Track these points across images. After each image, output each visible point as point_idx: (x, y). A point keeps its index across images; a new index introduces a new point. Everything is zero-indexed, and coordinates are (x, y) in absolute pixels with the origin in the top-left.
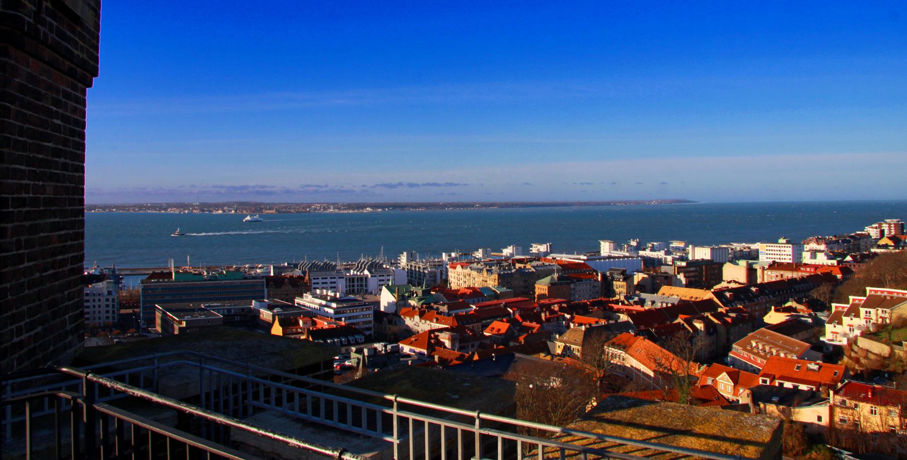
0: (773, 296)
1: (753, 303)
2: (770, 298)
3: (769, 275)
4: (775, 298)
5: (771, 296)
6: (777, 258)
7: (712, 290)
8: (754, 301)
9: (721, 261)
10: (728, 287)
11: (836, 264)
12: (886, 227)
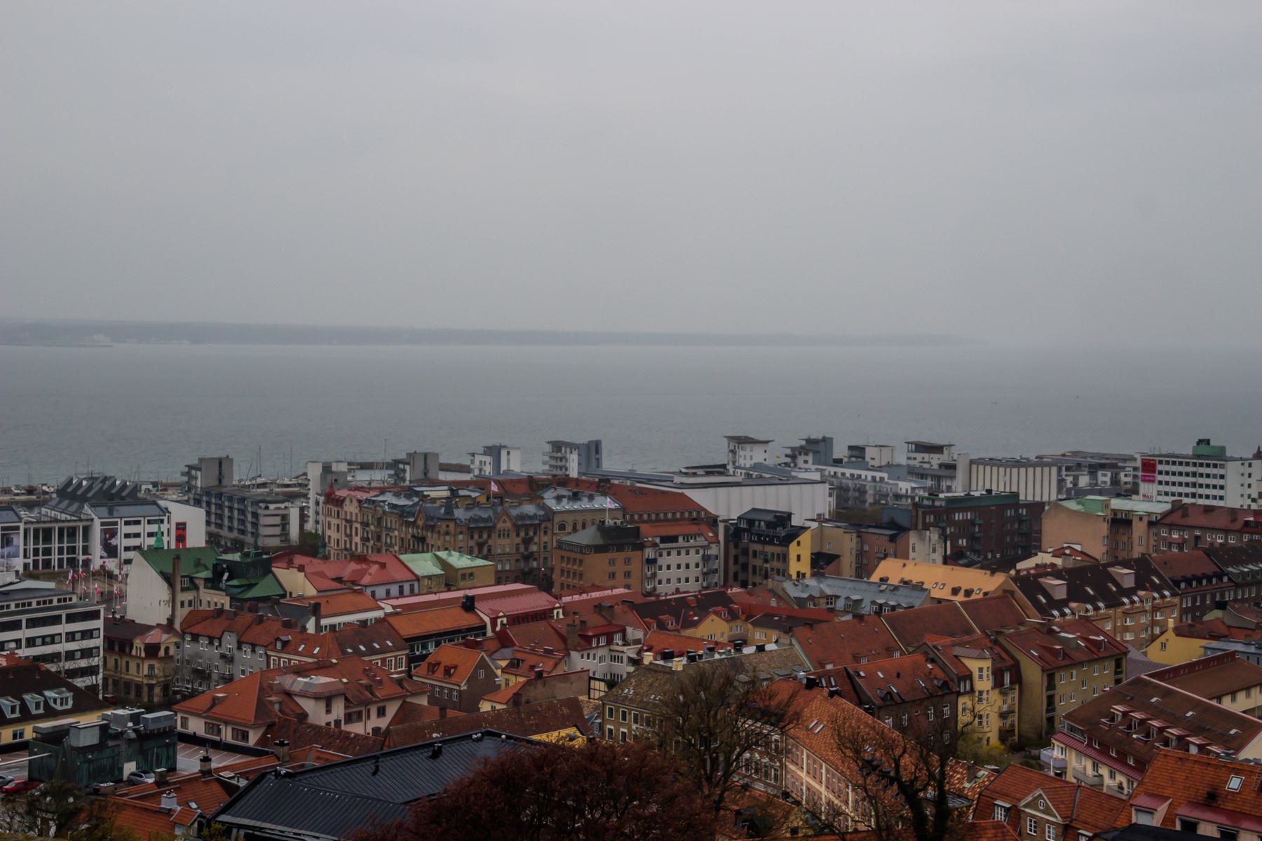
0: (1173, 595)
1: (1119, 610)
2: (1163, 597)
3: (1164, 539)
4: (1176, 600)
5: (1167, 593)
8: (1124, 604)
9: (1038, 499)
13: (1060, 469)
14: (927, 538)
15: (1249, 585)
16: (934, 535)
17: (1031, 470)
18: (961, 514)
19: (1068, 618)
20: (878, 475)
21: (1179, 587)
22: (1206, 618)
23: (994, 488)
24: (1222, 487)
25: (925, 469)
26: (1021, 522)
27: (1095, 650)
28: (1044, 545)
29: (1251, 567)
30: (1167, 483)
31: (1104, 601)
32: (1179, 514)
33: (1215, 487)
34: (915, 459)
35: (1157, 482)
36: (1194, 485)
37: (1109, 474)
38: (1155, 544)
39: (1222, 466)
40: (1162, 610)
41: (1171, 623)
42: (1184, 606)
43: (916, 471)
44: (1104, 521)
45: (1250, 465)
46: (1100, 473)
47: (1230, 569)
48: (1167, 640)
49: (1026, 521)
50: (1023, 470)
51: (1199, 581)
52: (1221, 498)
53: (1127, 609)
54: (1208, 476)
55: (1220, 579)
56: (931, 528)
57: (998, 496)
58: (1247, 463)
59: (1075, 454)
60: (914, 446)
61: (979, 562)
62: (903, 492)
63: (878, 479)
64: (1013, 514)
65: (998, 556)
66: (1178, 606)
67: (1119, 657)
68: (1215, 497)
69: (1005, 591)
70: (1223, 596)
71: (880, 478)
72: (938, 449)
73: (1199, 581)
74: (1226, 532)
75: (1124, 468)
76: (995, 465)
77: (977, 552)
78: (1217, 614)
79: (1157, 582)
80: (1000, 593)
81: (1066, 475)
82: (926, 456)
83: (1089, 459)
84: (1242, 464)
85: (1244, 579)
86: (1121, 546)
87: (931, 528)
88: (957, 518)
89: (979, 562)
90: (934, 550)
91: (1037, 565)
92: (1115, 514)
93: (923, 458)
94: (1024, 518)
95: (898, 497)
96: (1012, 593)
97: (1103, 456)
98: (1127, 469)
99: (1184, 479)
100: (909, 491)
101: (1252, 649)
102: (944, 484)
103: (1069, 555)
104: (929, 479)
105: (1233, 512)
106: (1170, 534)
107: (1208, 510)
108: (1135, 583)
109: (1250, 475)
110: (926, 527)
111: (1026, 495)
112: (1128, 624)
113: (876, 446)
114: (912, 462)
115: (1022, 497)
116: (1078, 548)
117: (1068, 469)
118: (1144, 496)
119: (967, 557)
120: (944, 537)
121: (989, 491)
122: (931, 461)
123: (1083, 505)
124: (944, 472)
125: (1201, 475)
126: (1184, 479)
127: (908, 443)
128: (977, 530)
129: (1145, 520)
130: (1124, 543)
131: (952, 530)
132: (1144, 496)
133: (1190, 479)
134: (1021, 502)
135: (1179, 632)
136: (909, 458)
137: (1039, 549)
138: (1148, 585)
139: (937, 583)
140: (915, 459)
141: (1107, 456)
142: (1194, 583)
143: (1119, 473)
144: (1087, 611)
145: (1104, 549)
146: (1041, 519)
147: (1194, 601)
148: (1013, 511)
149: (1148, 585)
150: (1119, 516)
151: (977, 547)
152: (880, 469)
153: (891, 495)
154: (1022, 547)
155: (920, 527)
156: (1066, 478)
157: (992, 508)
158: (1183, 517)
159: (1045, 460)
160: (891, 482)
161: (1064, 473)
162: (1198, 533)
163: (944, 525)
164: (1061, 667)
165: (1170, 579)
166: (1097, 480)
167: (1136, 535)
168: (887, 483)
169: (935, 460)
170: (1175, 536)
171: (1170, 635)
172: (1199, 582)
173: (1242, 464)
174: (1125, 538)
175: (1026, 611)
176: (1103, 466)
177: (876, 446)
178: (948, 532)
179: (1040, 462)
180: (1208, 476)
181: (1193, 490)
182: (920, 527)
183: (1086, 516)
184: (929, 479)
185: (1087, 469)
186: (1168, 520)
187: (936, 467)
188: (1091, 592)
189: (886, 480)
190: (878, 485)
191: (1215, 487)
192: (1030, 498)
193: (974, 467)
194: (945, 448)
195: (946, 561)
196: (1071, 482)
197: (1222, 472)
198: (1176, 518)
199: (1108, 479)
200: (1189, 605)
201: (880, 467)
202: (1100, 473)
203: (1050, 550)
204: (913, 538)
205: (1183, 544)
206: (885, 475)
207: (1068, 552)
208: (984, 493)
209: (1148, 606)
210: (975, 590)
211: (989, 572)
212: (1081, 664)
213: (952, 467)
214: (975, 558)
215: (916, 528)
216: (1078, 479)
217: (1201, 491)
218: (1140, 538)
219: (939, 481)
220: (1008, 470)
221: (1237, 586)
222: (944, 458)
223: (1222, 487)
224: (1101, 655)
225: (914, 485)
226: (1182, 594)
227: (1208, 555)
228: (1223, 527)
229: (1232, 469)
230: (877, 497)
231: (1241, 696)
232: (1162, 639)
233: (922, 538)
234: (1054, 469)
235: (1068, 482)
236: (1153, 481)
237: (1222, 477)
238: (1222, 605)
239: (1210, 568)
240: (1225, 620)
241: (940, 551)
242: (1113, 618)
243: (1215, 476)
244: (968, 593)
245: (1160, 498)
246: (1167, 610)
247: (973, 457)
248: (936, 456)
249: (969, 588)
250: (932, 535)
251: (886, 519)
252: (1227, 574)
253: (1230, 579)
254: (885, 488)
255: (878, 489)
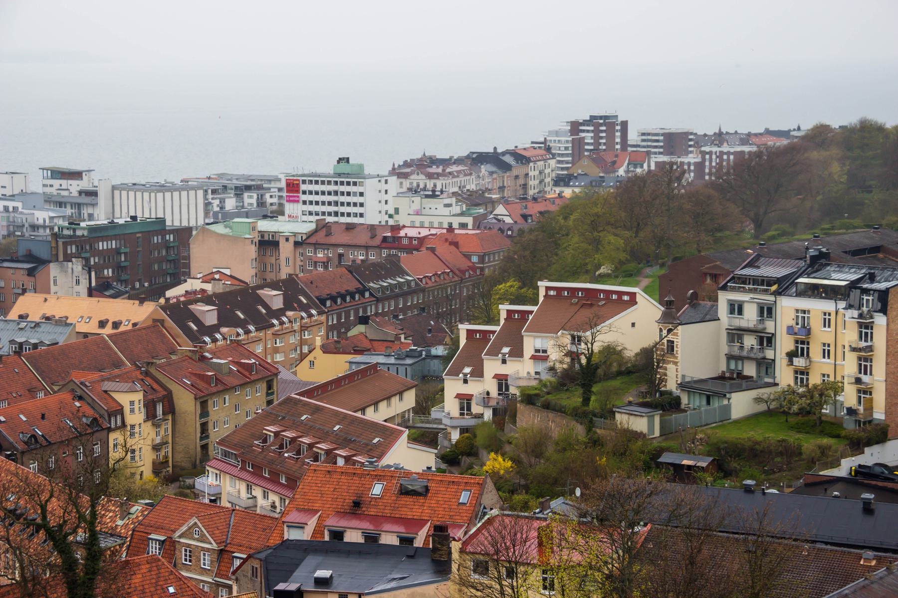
0: (319, 313)
1: (269, 332)
2: (310, 316)
3: (310, 258)
4: (323, 318)
5: (314, 312)
6: (330, 214)
7: (162, 301)
8: (273, 325)
9: (185, 224)
10: (203, 291)
11: (470, 226)
12: (588, 131)
13: (206, 191)
14: (70, 270)
15: (388, 298)
16: (77, 266)
17: (176, 194)
18: (105, 243)
19: (219, 343)
20: (11, 204)
21: (325, 306)
22: (350, 334)
23: (139, 215)
24: (362, 205)
25: (63, 197)
26: (168, 248)
27: (247, 374)
28: (194, 271)
29: (390, 281)
30: (311, 203)
31: (254, 323)
32: (322, 233)
33: (355, 205)
34: (51, 186)
35: (301, 202)
36: (336, 203)
37: (255, 196)
38: (302, 263)
39: (361, 184)
40: (309, 329)
41: (318, 341)
42: (330, 323)
43: (54, 199)
44: (252, 241)
45: (386, 182)
46: (246, 195)
47: (371, 284)
48: (315, 358)
49: (173, 247)
50: (168, 195)
51: (344, 299)
52: (361, 215)
53: (278, 331)
54: (349, 194)
55: (362, 295)
56: (73, 260)
57: (144, 223)
58: (383, 180)
59: (221, 176)
60: (49, 172)
61: (127, 292)
62: (41, 222)
63: (11, 209)
64: (160, 241)
65: (146, 284)
66: (325, 324)
67: (270, 378)
68: (355, 215)
69: (155, 321)
70: (365, 311)
71: (13, 207)
72: (76, 175)
73: (344, 299)
74: (367, 248)
75: (269, 189)
76: (139, 190)
77: (125, 282)
78: (361, 328)
79: (305, 301)
80: (150, 323)
81: (213, 199)
82: (65, 183)
83: (235, 182)
84: (380, 181)
85: (383, 293)
86: (269, 269)
87: (73, 260)
88: (101, 248)
89: (127, 292)
90: (78, 282)
91: (186, 291)
92: (262, 236)
93: (61, 185)
94: (171, 245)
95: (34, 227)
96: (162, 322)
97: (249, 178)
98: (272, 190)
99: (327, 198)
100: (47, 221)
101: (392, 360)
102: (85, 212)
103: (219, 280)
104: (69, 207)
105: (372, 228)
106: (315, 253)
107: (350, 227)
108: (284, 304)
109: (386, 192)
110: (68, 258)
111: (173, 221)
112: (278, 345)
113: (7, 173)
114: (48, 190)
115: (168, 223)
116: (227, 272)
117: (214, 192)
118: (290, 216)
119: (113, 288)
120: (88, 268)
121: (134, 218)
122: (69, 187)
123: (231, 228)
124: (84, 199)
125: (342, 194)
126: (327, 198)
127: (43, 169)
128: (123, 259)
129: (292, 240)
130: (272, 265)
131: (97, 260)
132: (290, 216)
133: (332, 198)
134: (167, 228)
135: (326, 349)
136: (44, 186)
137: (188, 275)
138: (296, 305)
139: (82, 317)
140: (51, 186)
141: (251, 178)
142: (339, 300)
143: (265, 195)
144: (238, 335)
145: (253, 272)
146: (189, 245)
147: (339, 318)
148: (160, 237)
149: (296, 305)
150: (266, 238)
151: (124, 277)
152: (12, 197)
153: (27, 225)
154: (170, 274)
155: (61, 258)
156: (212, 201)
157: (138, 235)
158: (326, 236)
159: (190, 183)
160: (25, 211)
161: (210, 196)
162: (341, 251)
163: (87, 255)
164: (213, 394)
165: (316, 297)
166: (243, 202)
167: (283, 257)
168: (21, 213)
169: (75, 186)
170: (320, 255)
171: (318, 352)
172: (344, 299)
173: (380, 181)
174: (273, 260)
175: (177, 340)
176: (248, 188)
177: (7, 173)
178: (92, 263)
179: (186, 186)
180: (349, 194)
181: (335, 209)
182: (61, 258)
183: (235, 239)
184: (69, 207)
185: (233, 192)
186: (313, 240)
187: (75, 194)
188: (242, 316)
189: (20, 209)
190: (12, 215)
191: (355, 205)
192: (177, 223)
193: (117, 193)
194: (84, 174)
195: (91, 293)
196: (218, 206)
197: (361, 189)
198: (320, 237)
199: (254, 201)
200: (335, 322)
201: (13, 196)
202: (246, 195)
203: (199, 276)
204: (54, 270)
205: (328, 262)
206: (19, 205)
207: (217, 276)
208: (129, 219)
209: (296, 326)
210: (124, 322)
211: (137, 302)
212: (234, 388)
213: (93, 194)
214: (122, 288)
215: (57, 260)
216: (224, 202)
217: (342, 209)
218: (288, 259)
219: (79, 209)
220: (153, 195)
221: (378, 300)
222: (84, 184)
223: (362, 205)
224: (252, 378)
225: (52, 214)
226: (328, 311)
227: (351, 272)
228: (364, 244)
229: (370, 187)
230: (11, 228)
231: (383, 405)
232: (310, 357)
233: (64, 270)
234: (200, 193)
235: (215, 205)
236: (298, 201)
237: (361, 194)
238: (364, 320)
239: (353, 285)
240: (368, 335)
241: (84, 284)
242: (264, 340)
243: (355, 194)
244: (116, 325)
245: (305, 218)
246: (315, 328)
247: (114, 183)
248: (74, 183)
249: (116, 320)
250: (75, 267)
251: (22, 252)
252: (368, 290)
253: (371, 294)
254: (19, 219)
255: (11, 219)
